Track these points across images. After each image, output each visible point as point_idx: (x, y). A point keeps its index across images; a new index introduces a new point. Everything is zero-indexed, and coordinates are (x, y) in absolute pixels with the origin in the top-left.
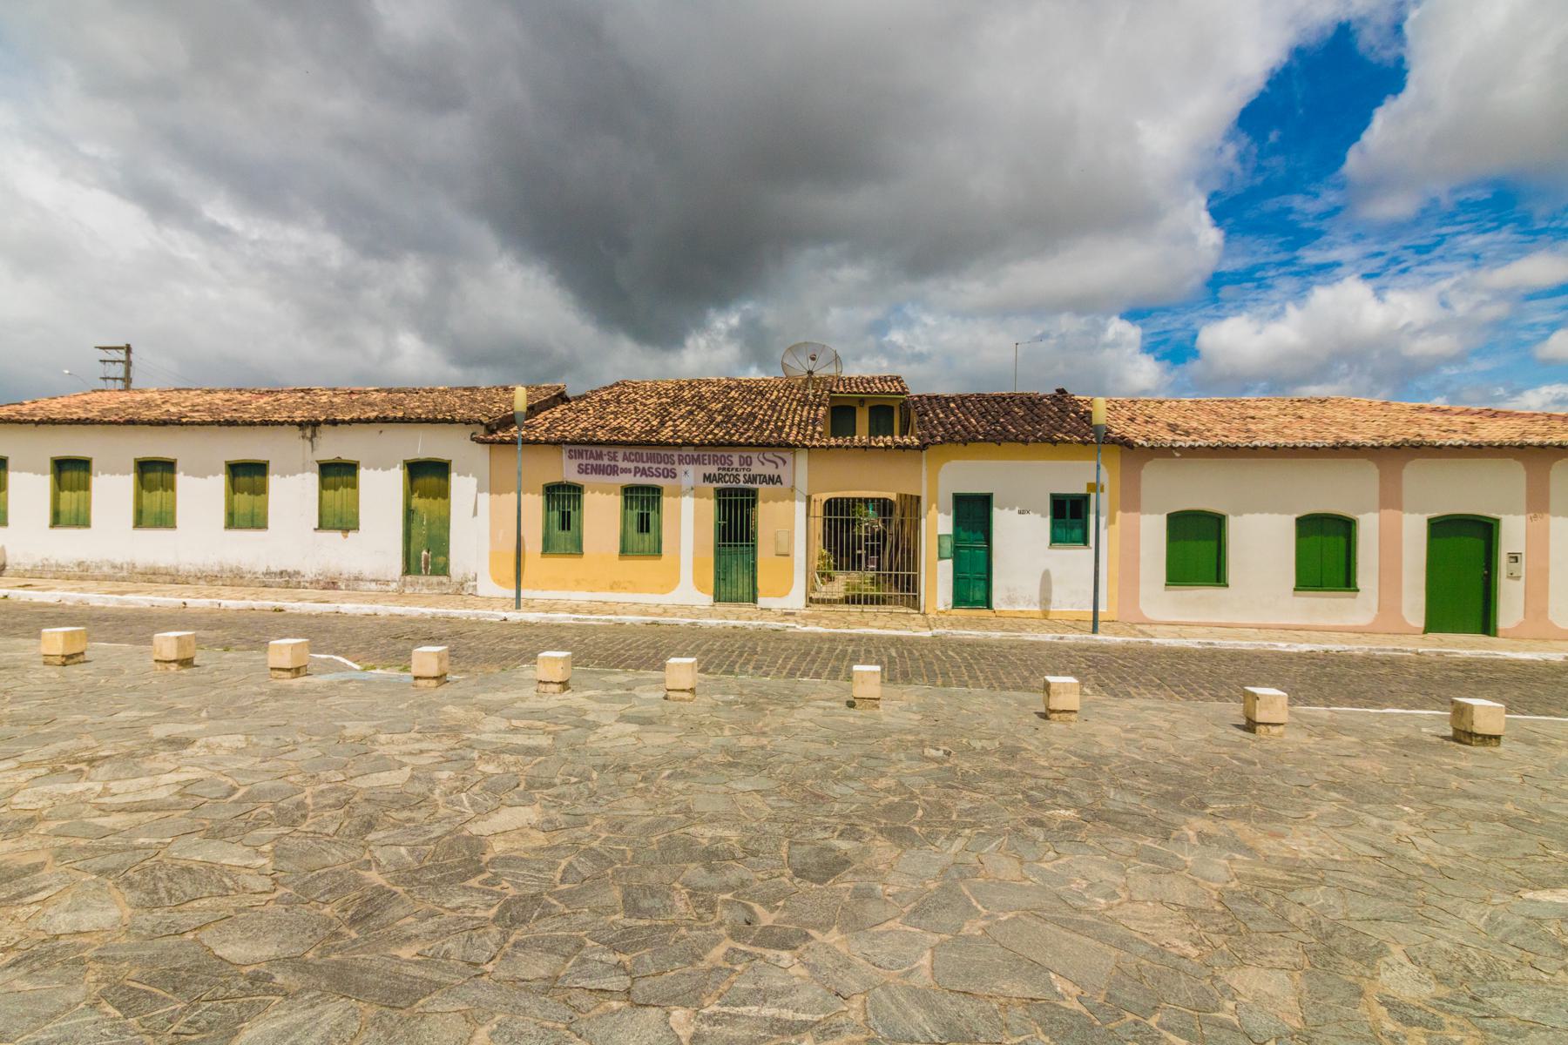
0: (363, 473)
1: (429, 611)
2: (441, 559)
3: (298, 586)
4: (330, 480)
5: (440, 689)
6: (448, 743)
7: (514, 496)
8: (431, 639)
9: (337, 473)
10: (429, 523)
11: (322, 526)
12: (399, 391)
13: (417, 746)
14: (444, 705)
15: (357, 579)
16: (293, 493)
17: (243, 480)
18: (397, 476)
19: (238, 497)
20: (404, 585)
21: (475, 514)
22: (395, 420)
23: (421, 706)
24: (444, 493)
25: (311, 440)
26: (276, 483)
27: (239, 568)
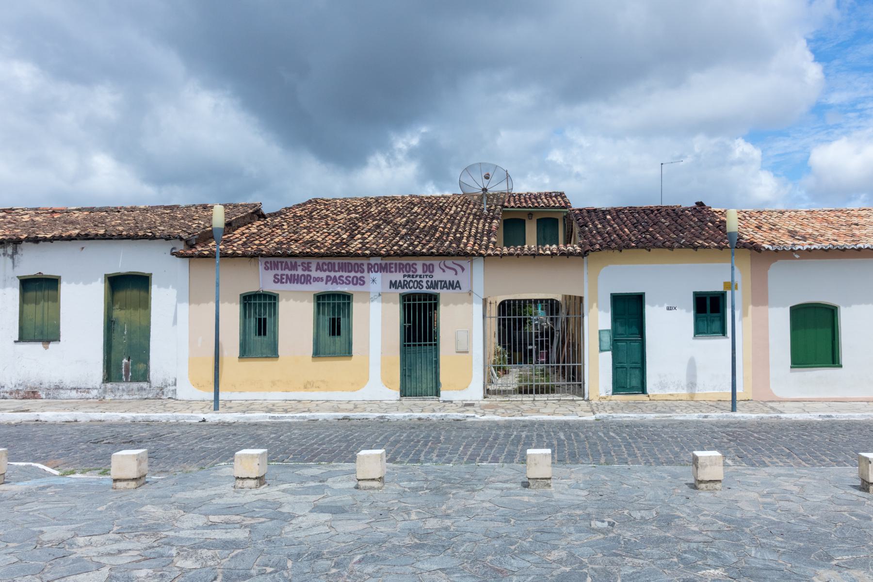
1: (129, 416)
5: (140, 490)
6: (146, 541)
8: (132, 443)
10: (129, 332)
12: (101, 210)
13: (116, 547)
14: (143, 505)
18: (98, 290)
20: (105, 391)
22: (96, 237)
23: (120, 507)
25: (12, 257)
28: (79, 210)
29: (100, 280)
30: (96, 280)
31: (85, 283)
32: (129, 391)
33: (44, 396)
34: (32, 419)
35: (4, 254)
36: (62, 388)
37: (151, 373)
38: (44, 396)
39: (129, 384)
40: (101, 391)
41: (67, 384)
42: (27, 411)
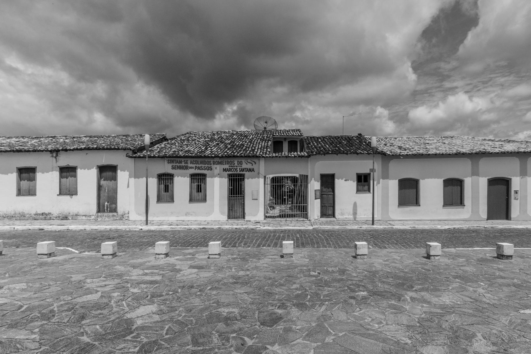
0: (79, 172)
4: (64, 174)
7: (145, 179)
11: (60, 194)
16: (47, 180)
21: (128, 187)
24: (114, 178)
27: (23, 213)
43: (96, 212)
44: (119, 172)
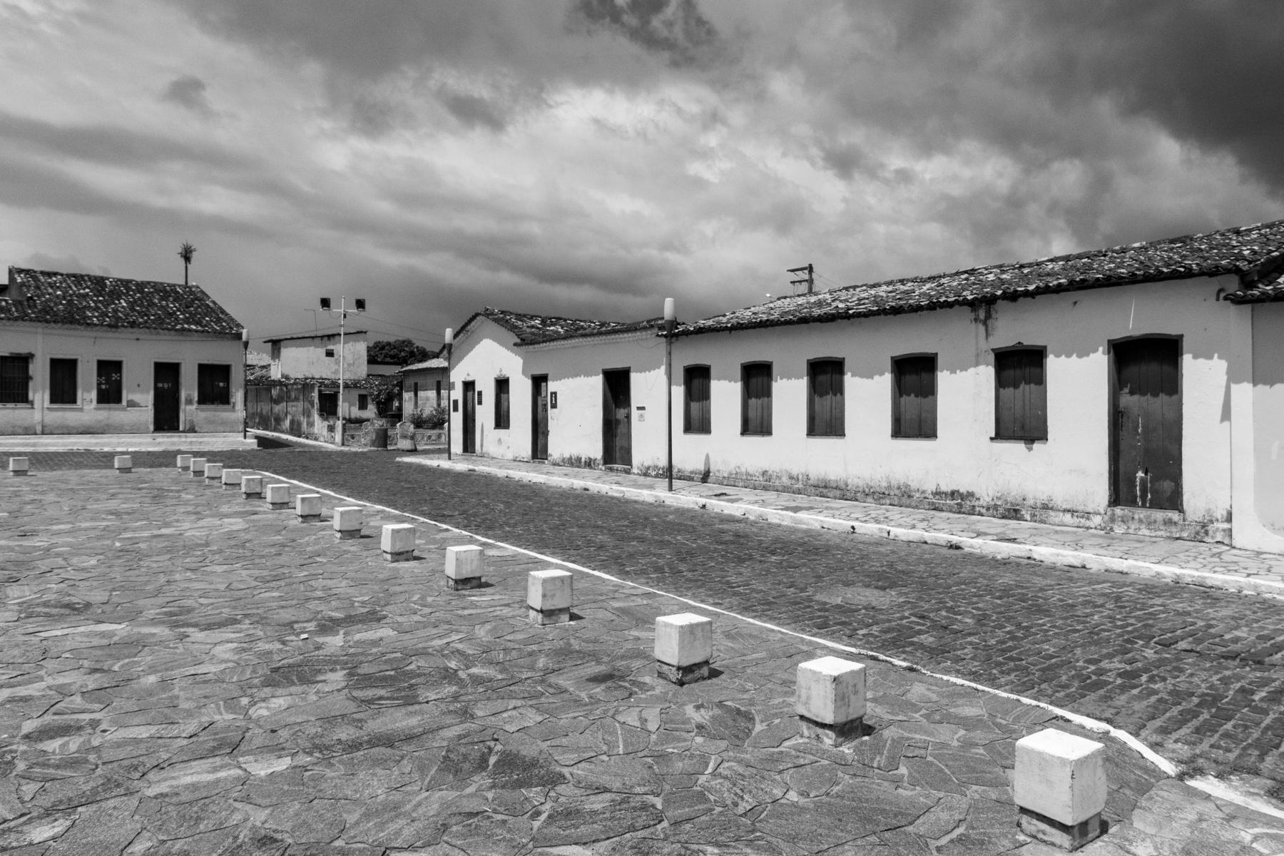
2: (1167, 485)
3: (972, 512)
9: (1020, 367)
15: (1046, 507)
17: (910, 379)
18: (1098, 364)
19: (904, 399)
20: (1112, 520)
21: (1226, 414)
24: (1172, 386)
26: (945, 380)
27: (907, 486)
28: (1051, 260)
29: (1101, 349)
30: (1096, 351)
31: (1080, 356)
32: (1150, 523)
33: (1028, 517)
34: (1023, 554)
35: (976, 320)
36: (1051, 509)
37: (1185, 498)
38: (1028, 517)
39: (1149, 512)
40: (1106, 518)
41: (1059, 503)
42: (1014, 540)
43: (1105, 501)
44: (1187, 361)
